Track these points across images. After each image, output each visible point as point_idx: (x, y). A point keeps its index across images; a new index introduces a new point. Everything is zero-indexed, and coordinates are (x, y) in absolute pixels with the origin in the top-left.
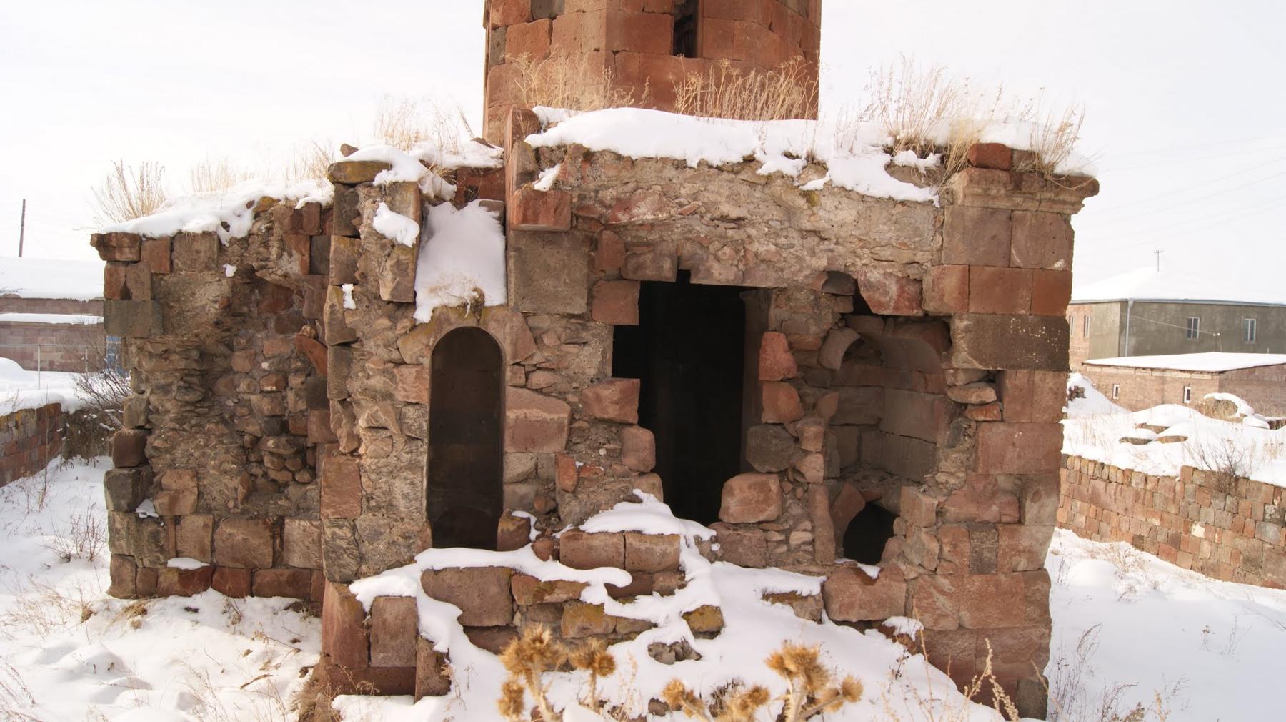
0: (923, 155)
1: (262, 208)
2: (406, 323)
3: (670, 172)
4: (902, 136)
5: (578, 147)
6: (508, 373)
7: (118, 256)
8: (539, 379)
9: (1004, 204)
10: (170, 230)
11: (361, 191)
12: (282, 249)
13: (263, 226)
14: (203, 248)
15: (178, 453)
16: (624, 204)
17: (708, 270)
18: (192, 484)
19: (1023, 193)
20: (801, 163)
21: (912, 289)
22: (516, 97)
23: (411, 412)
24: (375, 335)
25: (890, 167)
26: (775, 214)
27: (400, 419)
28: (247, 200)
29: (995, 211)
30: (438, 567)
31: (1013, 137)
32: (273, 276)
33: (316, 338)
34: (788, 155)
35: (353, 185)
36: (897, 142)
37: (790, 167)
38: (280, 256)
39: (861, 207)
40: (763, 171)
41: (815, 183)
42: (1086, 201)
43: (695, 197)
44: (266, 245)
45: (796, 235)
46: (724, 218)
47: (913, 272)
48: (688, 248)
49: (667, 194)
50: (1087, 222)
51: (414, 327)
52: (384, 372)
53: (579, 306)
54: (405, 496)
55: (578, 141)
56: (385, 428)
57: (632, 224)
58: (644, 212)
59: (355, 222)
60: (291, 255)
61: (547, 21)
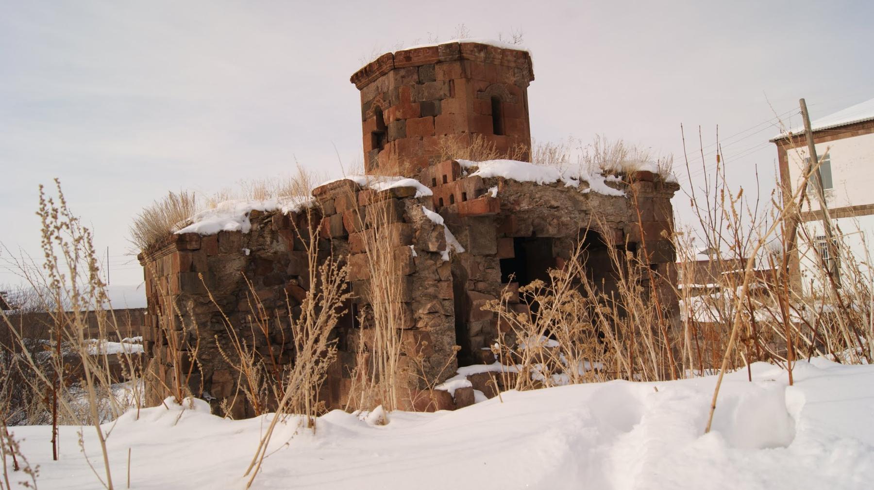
0: (617, 177)
1: (255, 216)
2: (439, 263)
3: (532, 188)
4: (607, 168)
5: (503, 178)
6: (467, 285)
7: (188, 247)
8: (481, 285)
9: (650, 195)
10: (216, 230)
11: (408, 202)
12: (273, 238)
13: (256, 226)
14: (235, 240)
15: (216, 362)
16: (517, 202)
17: (548, 230)
18: (230, 378)
19: (654, 189)
20: (578, 181)
21: (620, 233)
22: (416, 154)
23: (447, 303)
24: (429, 268)
25: (605, 182)
26: (569, 204)
27: (443, 306)
28: (244, 212)
29: (647, 199)
30: (471, 374)
31: (652, 169)
32: (269, 253)
33: (299, 285)
34: (572, 178)
35: (402, 198)
36: (606, 171)
37: (575, 184)
38: (272, 242)
39: (601, 199)
40: (566, 186)
41: (587, 191)
42: (675, 193)
43: (540, 198)
44: (264, 237)
45: (577, 212)
46: (552, 207)
47: (621, 226)
48: (537, 221)
49: (532, 198)
50: (678, 201)
51: (445, 263)
52: (434, 285)
53: (493, 252)
54: (449, 344)
55: (500, 174)
56: (436, 312)
57: (520, 211)
58: (524, 206)
59: (404, 216)
60: (278, 242)
61: (432, 118)
